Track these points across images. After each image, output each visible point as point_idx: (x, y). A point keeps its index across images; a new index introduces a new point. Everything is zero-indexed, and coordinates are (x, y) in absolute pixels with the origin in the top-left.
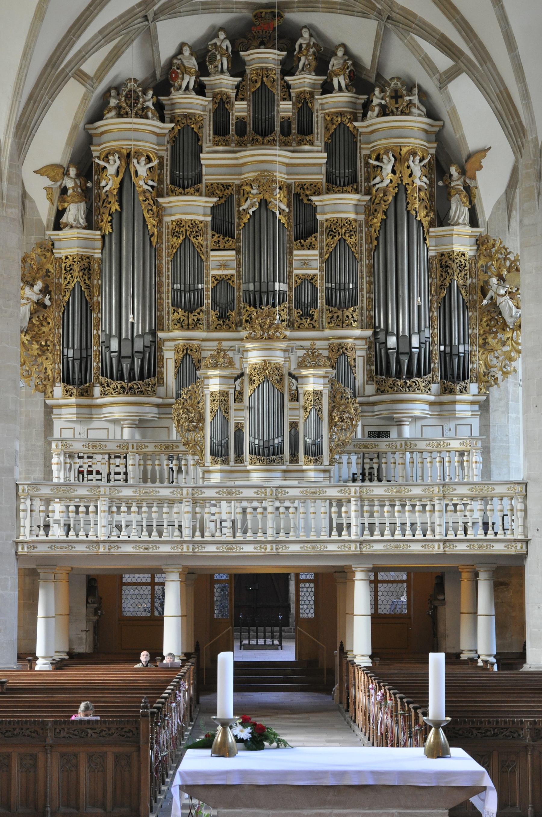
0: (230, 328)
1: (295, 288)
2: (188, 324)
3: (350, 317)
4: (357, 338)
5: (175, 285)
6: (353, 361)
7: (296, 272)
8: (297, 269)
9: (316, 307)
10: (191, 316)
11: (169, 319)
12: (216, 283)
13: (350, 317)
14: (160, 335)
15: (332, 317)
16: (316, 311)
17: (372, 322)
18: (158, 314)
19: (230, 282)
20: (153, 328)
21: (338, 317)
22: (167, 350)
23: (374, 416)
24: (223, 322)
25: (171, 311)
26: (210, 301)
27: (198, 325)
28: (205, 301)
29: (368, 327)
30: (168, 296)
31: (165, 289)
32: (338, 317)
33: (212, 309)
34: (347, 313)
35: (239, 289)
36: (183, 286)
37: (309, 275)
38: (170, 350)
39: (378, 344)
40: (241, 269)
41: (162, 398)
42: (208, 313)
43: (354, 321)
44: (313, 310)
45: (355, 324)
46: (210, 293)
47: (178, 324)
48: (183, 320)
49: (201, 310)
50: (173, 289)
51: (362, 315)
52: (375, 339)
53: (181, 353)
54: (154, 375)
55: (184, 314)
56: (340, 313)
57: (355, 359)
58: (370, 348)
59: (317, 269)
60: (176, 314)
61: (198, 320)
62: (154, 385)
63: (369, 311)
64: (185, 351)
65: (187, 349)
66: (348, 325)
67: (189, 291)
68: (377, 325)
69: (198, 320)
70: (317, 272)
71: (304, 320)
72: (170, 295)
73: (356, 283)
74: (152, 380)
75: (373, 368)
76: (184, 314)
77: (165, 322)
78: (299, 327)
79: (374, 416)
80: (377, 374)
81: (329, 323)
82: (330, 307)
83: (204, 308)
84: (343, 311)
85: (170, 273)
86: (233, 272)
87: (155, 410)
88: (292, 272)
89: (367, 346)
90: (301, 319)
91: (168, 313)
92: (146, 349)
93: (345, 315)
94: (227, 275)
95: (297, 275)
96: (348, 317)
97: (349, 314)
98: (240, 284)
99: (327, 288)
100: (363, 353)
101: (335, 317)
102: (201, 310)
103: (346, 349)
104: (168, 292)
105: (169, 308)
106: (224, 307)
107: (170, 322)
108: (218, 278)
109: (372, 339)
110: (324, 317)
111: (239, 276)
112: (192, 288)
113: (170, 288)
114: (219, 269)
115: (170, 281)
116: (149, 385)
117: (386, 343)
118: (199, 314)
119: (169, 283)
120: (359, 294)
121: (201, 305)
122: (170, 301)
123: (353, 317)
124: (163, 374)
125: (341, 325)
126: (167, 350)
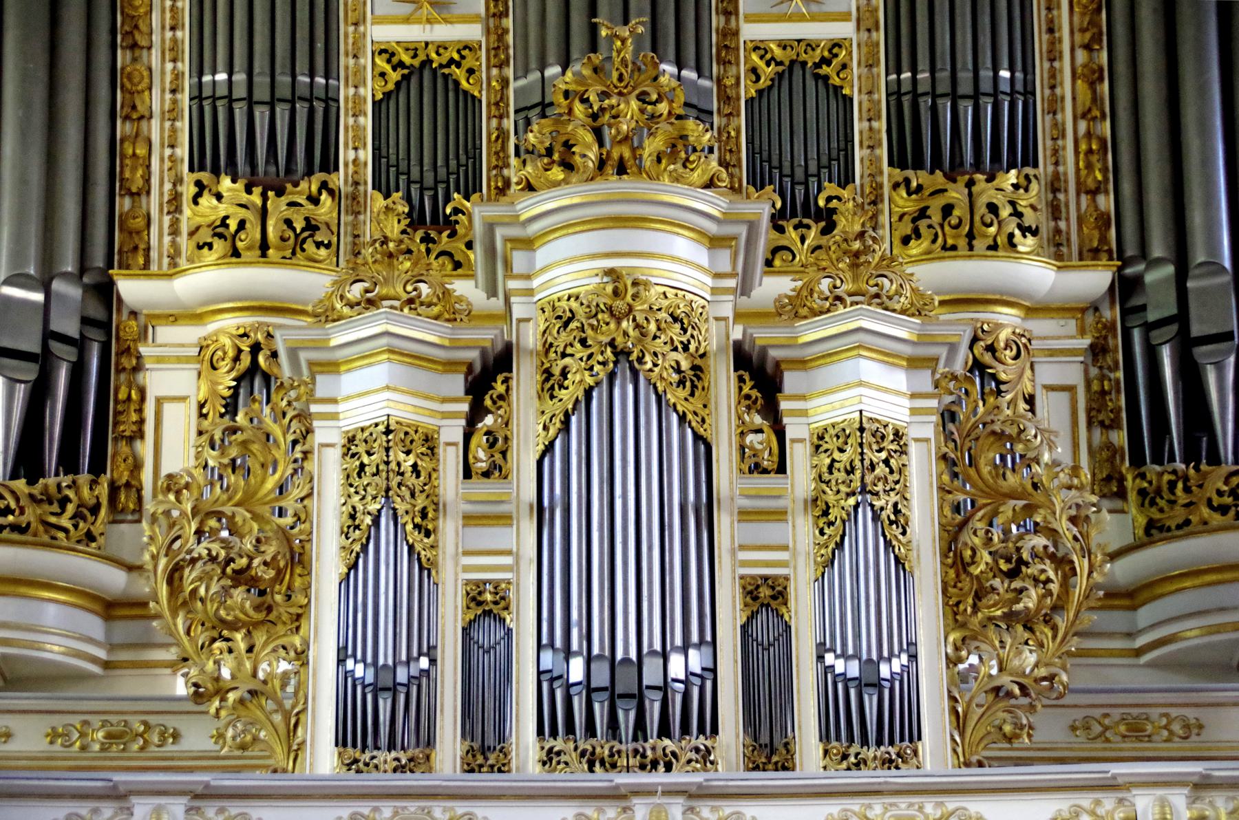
0: (457, 265)
1: (750, 101)
2: (264, 246)
3: (1005, 212)
4: (1036, 309)
5: (207, 78)
6: (1022, 406)
7: (750, 32)
8: (753, 18)
9: (846, 179)
10: (278, 207)
11: (175, 231)
12: (394, 76)
13: (1005, 212)
14: (130, 289)
15: (923, 213)
16: (845, 194)
17: (1104, 239)
18: (124, 204)
19: (460, 74)
20: (100, 262)
21: (947, 210)
22: (160, 359)
23: (1139, 652)
24: (426, 239)
25: (189, 190)
26: (367, 155)
27: (310, 246)
28: (345, 155)
29: (1091, 254)
30: (174, 130)
31: (157, 100)
32: (947, 210)
33: (376, 186)
34: (986, 192)
35: (499, 103)
36: (240, 77)
37: (811, 46)
38: (179, 359)
39: (1137, 335)
40: (509, 23)
41: (131, 568)
42: (355, 204)
43: (1025, 230)
44: (831, 189)
45: (1026, 244)
46: (367, 122)
47: (218, 245)
48: (242, 225)
49: (324, 185)
50: (198, 97)
51: (1055, 211)
52: (1125, 313)
53: (224, 366)
54: (98, 467)
55: (244, 198)
56: (957, 193)
57: (1030, 400)
58: (1097, 351)
59: (845, 17)
60: (207, 201)
61: (311, 226)
62: (95, 510)
63: (1094, 193)
64: (246, 361)
65: (256, 349)
66: (994, 247)
67: (272, 104)
68: (1130, 252)
69: (311, 226)
70: (845, 30)
71: (793, 234)
72: (184, 125)
73: (1029, 68)
74: (85, 488)
75: (1120, 438)
76: (244, 198)
77: (159, 238)
78: (769, 263)
79: (1139, 652)
80: (1137, 460)
81: (906, 241)
82: (910, 173)
83: (339, 180)
84: (970, 184)
85: (184, 35)
86: (473, 32)
87: (94, 625)
88: (736, 33)
89: (1086, 342)
90: (781, 230)
91: (176, 198)
92: (55, 346)
93: (981, 202)
94: (441, 47)
95: (759, 47)
96: (993, 208)
97: (999, 199)
98: (505, 83)
99: (895, 93)
100: (1073, 373)
101: (936, 218)
102: (324, 185)
103: (991, 349)
104: (173, 114)
105: (178, 181)
106: (429, 179)
107: (183, 240)
108: (406, 59)
109: (1112, 314)
110: (884, 219)
111: (498, 47)
112: (284, 91)
113: (185, 98)
114: (407, 20)
115: (184, 66)
116: (64, 501)
117: (1182, 317)
118: (315, 200)
119: (177, 76)
120: (1043, 123)
121: (329, 164)
122: (183, 152)
123: (1017, 214)
124: (137, 466)
125: (962, 243)
126: (160, 359)
